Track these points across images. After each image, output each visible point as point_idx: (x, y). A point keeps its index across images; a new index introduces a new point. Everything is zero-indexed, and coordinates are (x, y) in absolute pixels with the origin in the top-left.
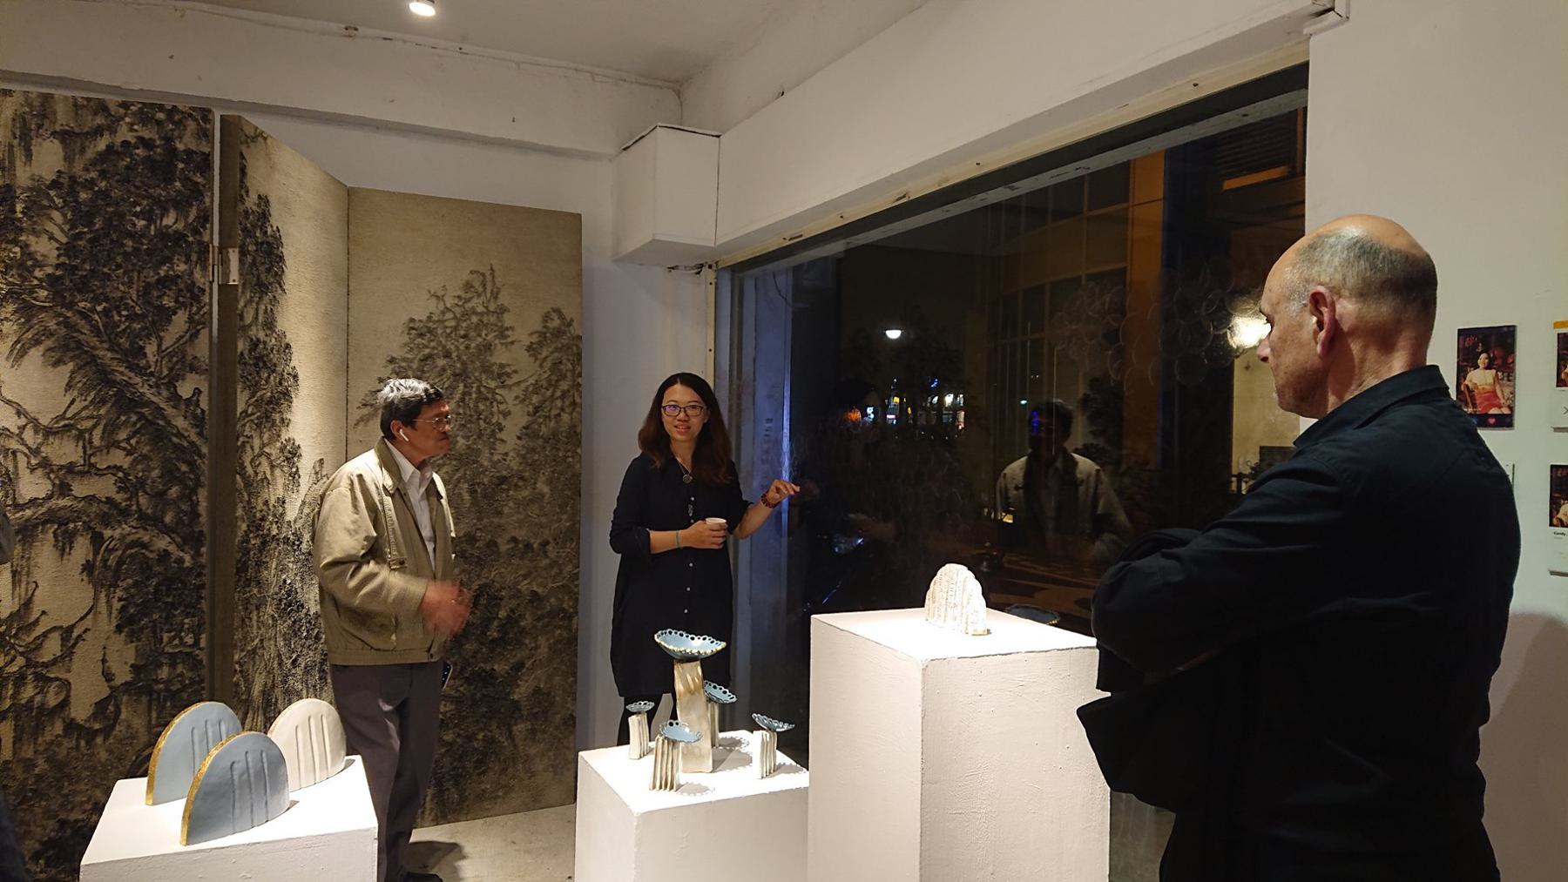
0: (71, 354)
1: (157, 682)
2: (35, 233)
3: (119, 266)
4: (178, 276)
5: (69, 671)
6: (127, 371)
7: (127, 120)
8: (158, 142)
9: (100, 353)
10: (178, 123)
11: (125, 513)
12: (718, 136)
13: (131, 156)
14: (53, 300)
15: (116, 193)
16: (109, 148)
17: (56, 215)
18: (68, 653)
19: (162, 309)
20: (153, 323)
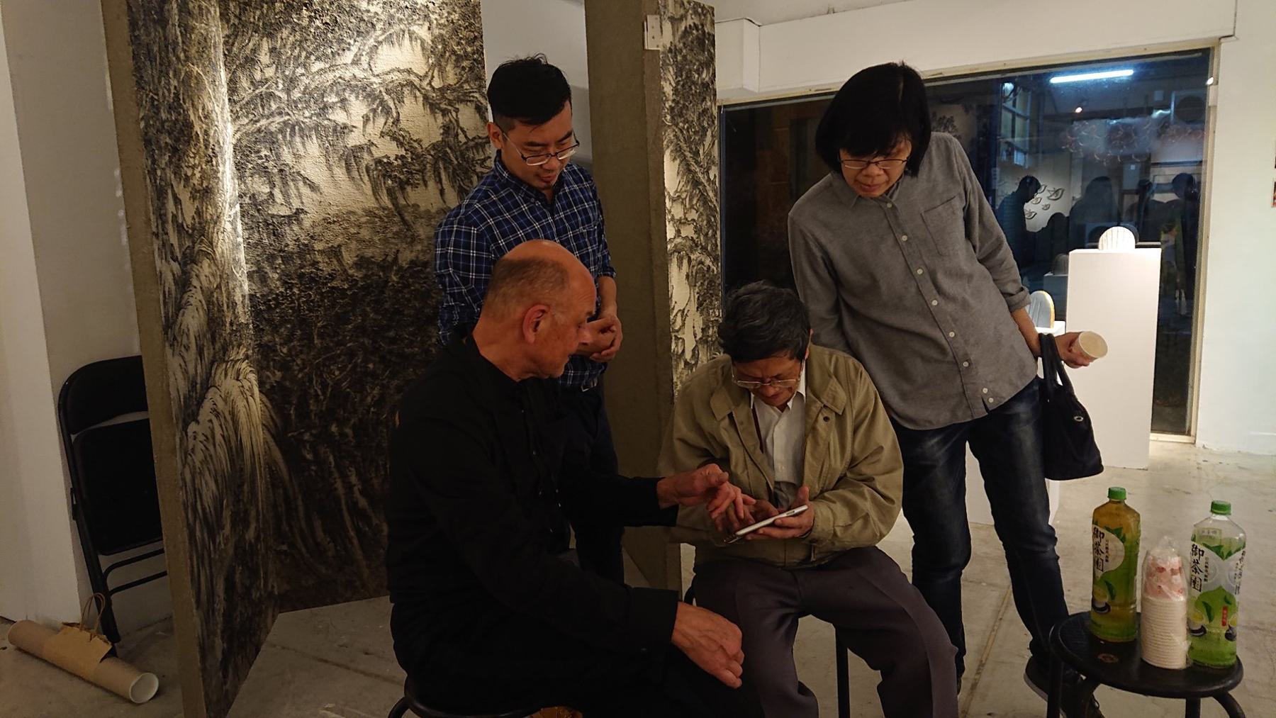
0: (678, 154)
1: (708, 336)
2: (665, 80)
3: (691, 102)
4: (708, 109)
5: (684, 333)
6: (696, 166)
7: (690, 12)
8: (700, 27)
9: (687, 153)
10: (705, 15)
11: (697, 246)
12: (759, 26)
13: (692, 34)
14: (672, 122)
15: (688, 57)
16: (686, 28)
17: (671, 69)
18: (684, 324)
19: (703, 127)
20: (701, 136)
